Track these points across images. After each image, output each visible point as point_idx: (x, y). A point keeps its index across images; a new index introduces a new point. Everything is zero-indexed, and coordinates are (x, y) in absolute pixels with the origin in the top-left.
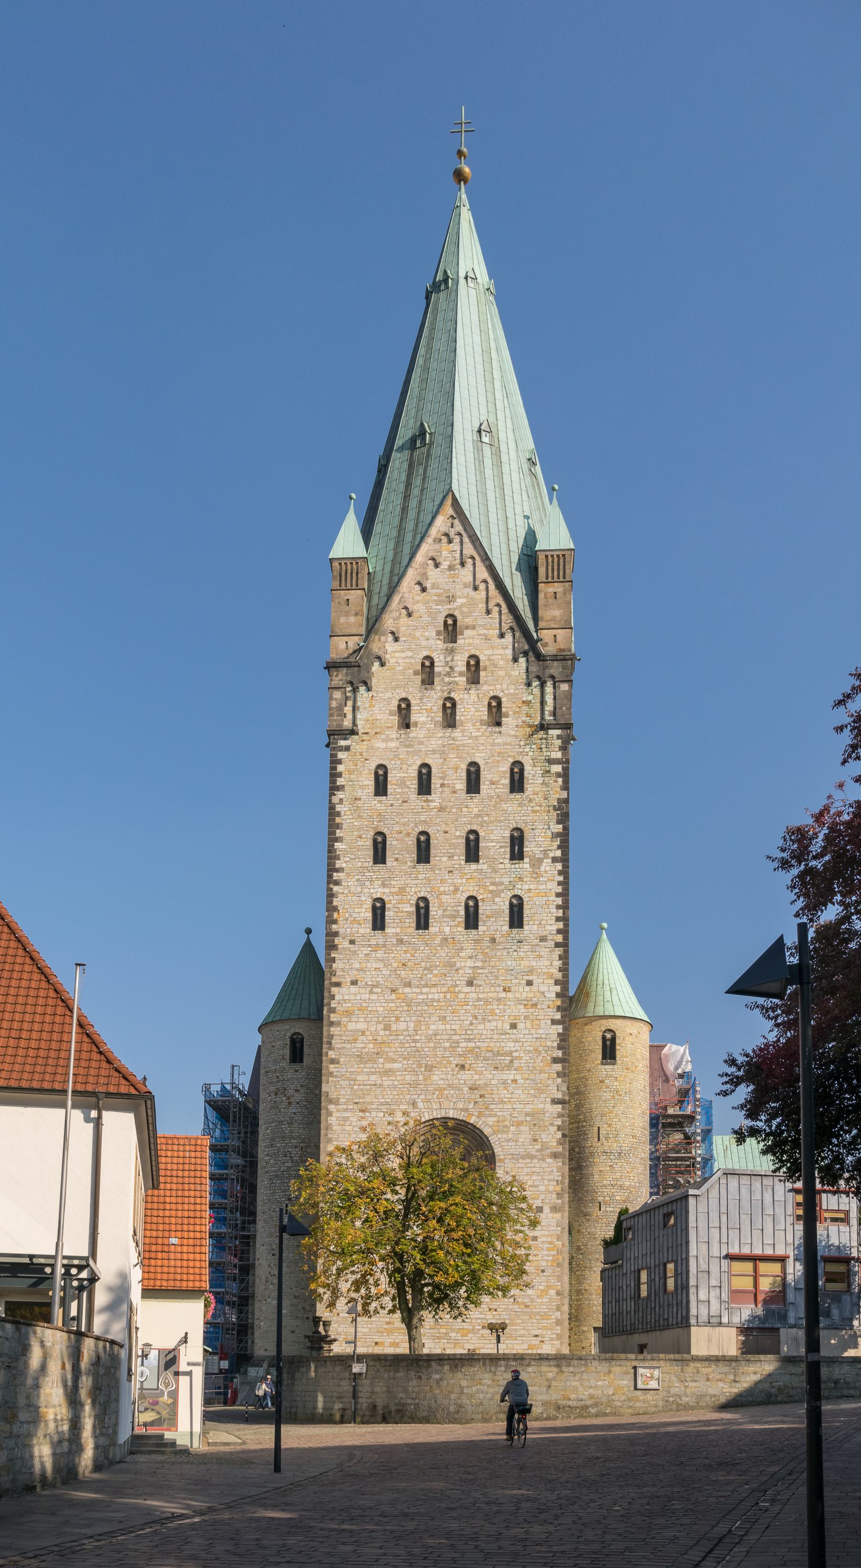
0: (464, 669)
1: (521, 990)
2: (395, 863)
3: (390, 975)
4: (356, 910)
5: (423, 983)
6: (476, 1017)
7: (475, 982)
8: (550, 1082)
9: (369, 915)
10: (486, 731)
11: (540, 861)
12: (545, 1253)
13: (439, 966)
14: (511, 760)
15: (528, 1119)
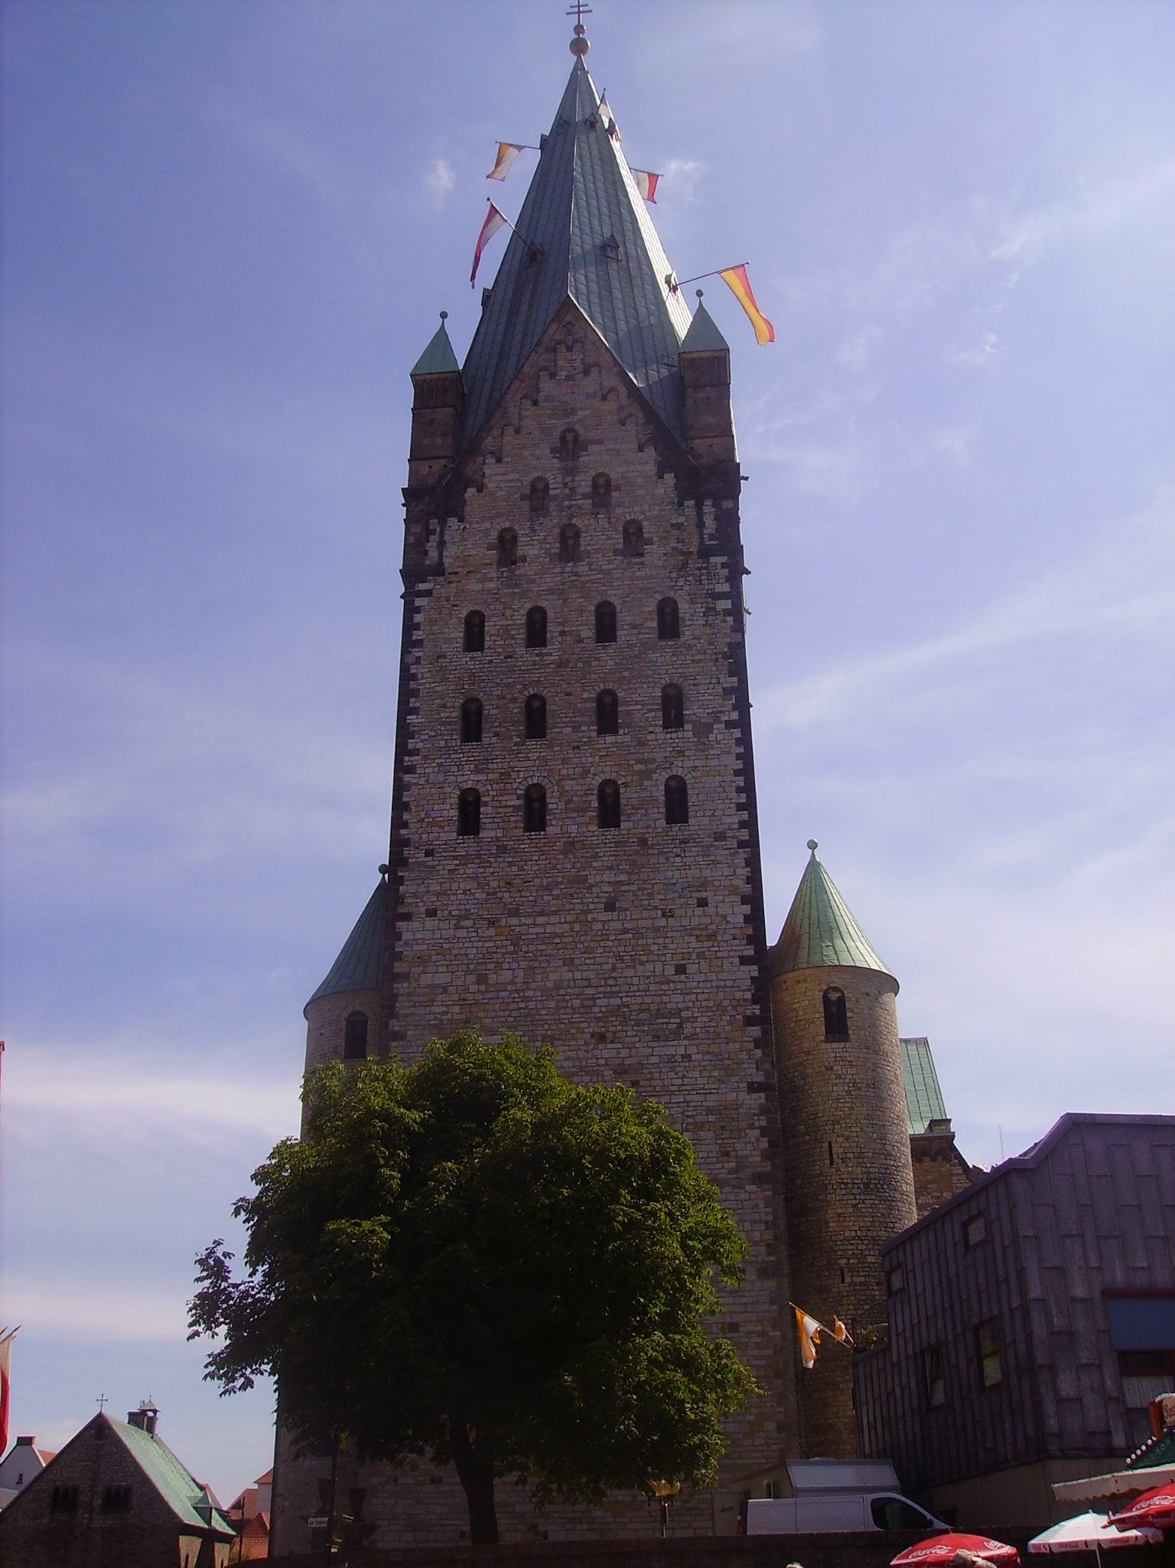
0: (589, 490)
1: (690, 913)
2: (494, 740)
3: (486, 900)
4: (436, 807)
5: (538, 909)
6: (620, 958)
7: (617, 905)
8: (744, 1056)
9: (455, 813)
10: (622, 562)
11: (709, 728)
12: (755, 1353)
13: (561, 883)
14: (659, 597)
15: (711, 1118)
